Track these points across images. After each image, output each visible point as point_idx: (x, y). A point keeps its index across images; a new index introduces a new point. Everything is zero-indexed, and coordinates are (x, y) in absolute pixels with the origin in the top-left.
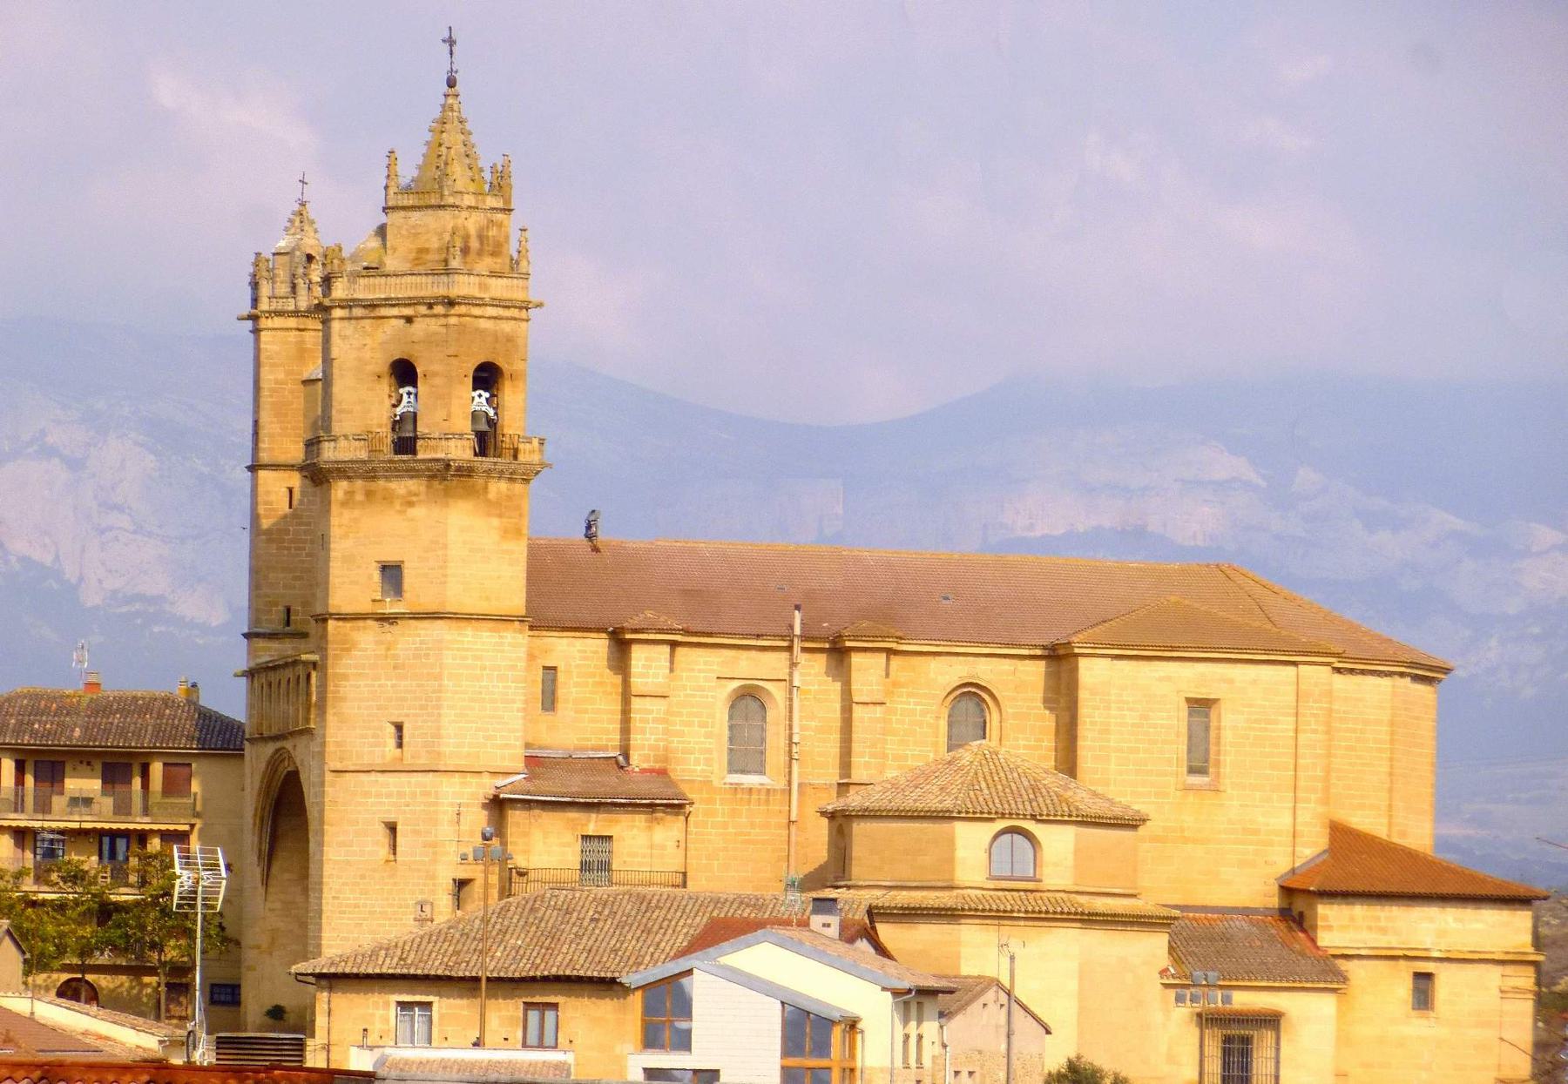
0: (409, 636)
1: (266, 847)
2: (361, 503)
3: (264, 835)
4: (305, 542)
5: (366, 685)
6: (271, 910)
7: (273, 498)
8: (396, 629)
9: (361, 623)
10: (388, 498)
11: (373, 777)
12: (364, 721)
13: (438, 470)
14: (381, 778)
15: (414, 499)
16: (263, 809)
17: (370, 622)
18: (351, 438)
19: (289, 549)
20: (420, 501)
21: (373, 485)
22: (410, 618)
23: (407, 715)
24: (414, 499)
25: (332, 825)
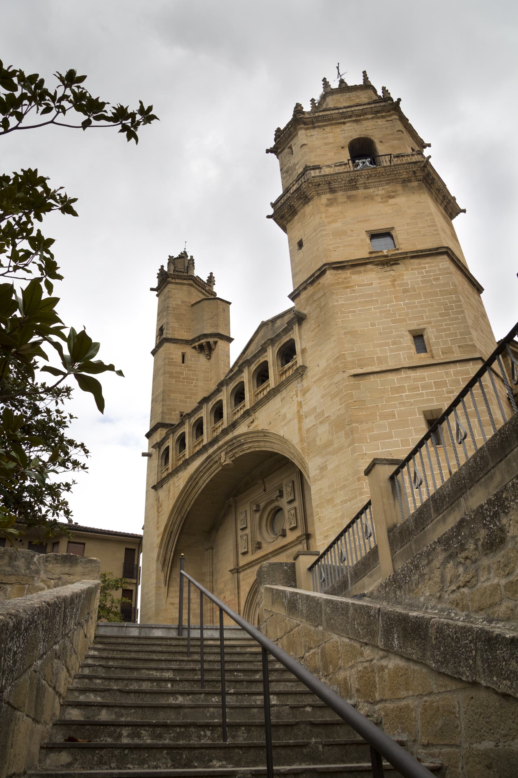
0: (412, 269)
1: (171, 555)
2: (345, 202)
3: (169, 548)
4: (193, 379)
5: (374, 308)
6: (172, 604)
7: (174, 356)
8: (400, 269)
9: (362, 269)
10: (370, 198)
11: (403, 374)
12: (380, 334)
13: (414, 172)
14: (412, 374)
15: (393, 194)
16: (173, 524)
17: (369, 267)
18: (333, 166)
19: (183, 382)
20: (398, 195)
21: (354, 193)
22: (412, 257)
23: (429, 323)
24: (393, 194)
25: (361, 422)
